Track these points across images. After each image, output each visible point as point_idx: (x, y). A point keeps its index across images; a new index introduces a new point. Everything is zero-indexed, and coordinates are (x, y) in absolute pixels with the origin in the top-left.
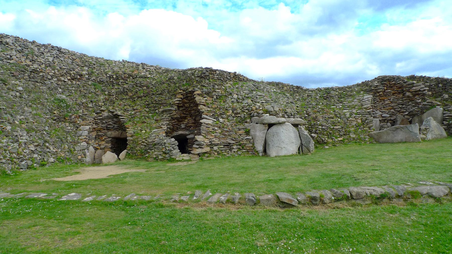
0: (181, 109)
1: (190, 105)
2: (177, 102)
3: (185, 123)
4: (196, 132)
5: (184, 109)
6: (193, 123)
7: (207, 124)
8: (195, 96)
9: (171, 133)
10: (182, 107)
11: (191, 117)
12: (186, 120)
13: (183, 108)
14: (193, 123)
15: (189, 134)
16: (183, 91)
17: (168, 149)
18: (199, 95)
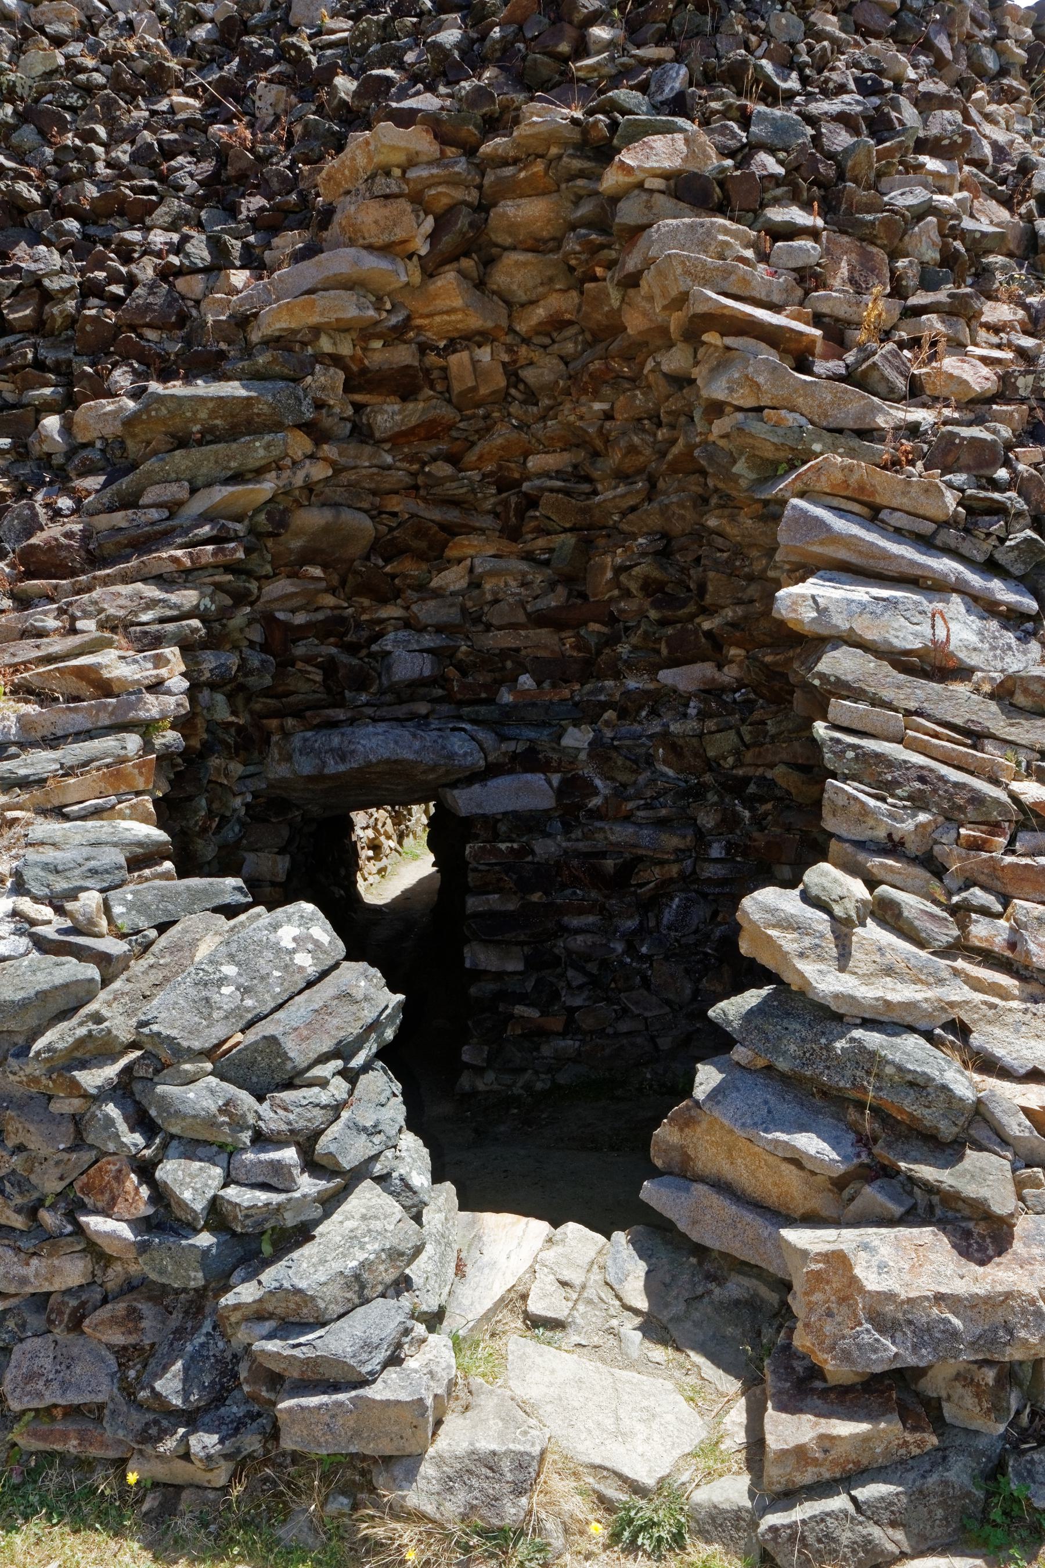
0: (389, 415)
1: (512, 373)
2: (349, 308)
3: (427, 611)
4: (577, 738)
5: (430, 430)
6: (540, 620)
7: (904, 662)
8: (628, 213)
9: (250, 743)
10: (404, 385)
11: (513, 534)
12: (453, 579)
13: (415, 412)
14: (540, 620)
15: (492, 771)
16: (442, 138)
17: (193, 1182)
18: (689, 190)
